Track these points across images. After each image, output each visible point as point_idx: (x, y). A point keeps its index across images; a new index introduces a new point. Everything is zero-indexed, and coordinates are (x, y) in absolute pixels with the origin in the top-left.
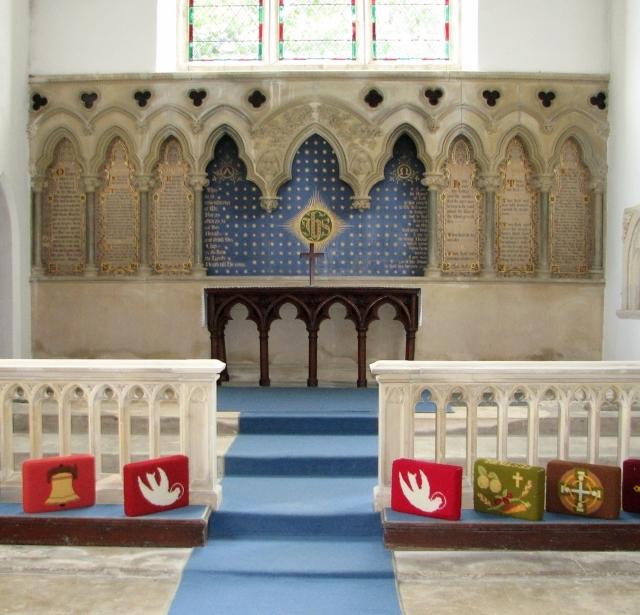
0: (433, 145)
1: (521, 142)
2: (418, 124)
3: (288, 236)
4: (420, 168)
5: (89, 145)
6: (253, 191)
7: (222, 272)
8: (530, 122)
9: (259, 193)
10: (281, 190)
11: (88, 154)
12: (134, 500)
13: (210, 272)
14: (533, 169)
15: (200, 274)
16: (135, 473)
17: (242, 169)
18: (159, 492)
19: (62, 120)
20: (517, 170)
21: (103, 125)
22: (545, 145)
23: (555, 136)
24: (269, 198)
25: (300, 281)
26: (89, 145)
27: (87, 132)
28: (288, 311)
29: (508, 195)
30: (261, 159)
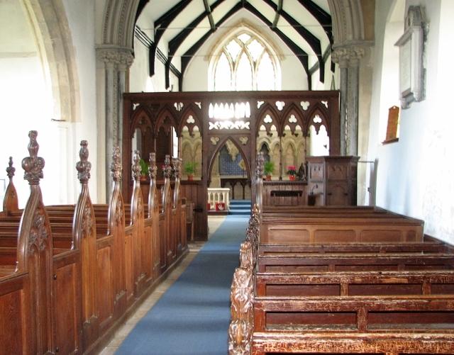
0: (271, 146)
1: (291, 145)
2: (267, 141)
3: (238, 167)
4: (268, 151)
5: (193, 146)
6: (230, 157)
7: (223, 175)
8: (293, 141)
9: (231, 157)
10: (237, 156)
11: (193, 148)
12: (217, 209)
13: (220, 175)
14: (294, 151)
15: (218, 175)
16: (217, 205)
17: (227, 151)
18: (221, 208)
19: (187, 140)
20: (290, 151)
21: (196, 141)
22: (296, 146)
23: (298, 144)
24: (234, 158)
25: (241, 177)
26: (193, 146)
27: (193, 143)
28: (238, 184)
29: (288, 157)
30: (232, 149)
